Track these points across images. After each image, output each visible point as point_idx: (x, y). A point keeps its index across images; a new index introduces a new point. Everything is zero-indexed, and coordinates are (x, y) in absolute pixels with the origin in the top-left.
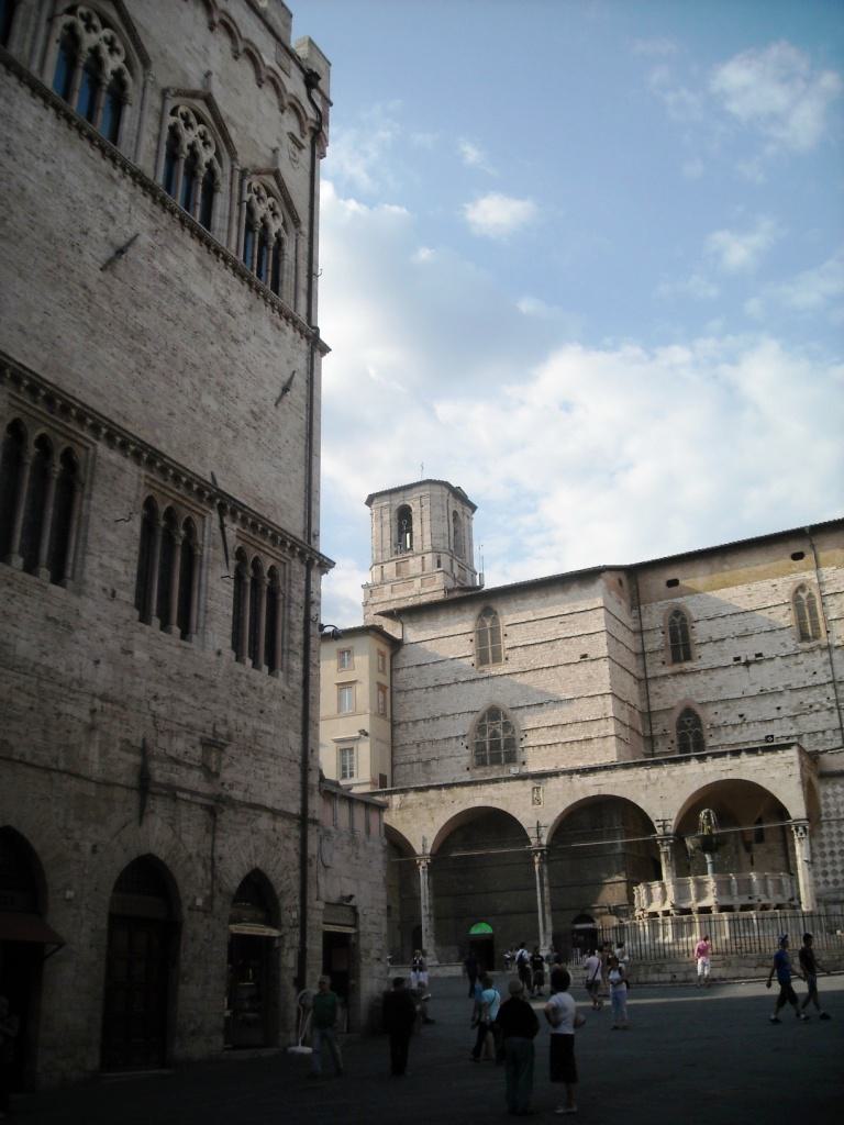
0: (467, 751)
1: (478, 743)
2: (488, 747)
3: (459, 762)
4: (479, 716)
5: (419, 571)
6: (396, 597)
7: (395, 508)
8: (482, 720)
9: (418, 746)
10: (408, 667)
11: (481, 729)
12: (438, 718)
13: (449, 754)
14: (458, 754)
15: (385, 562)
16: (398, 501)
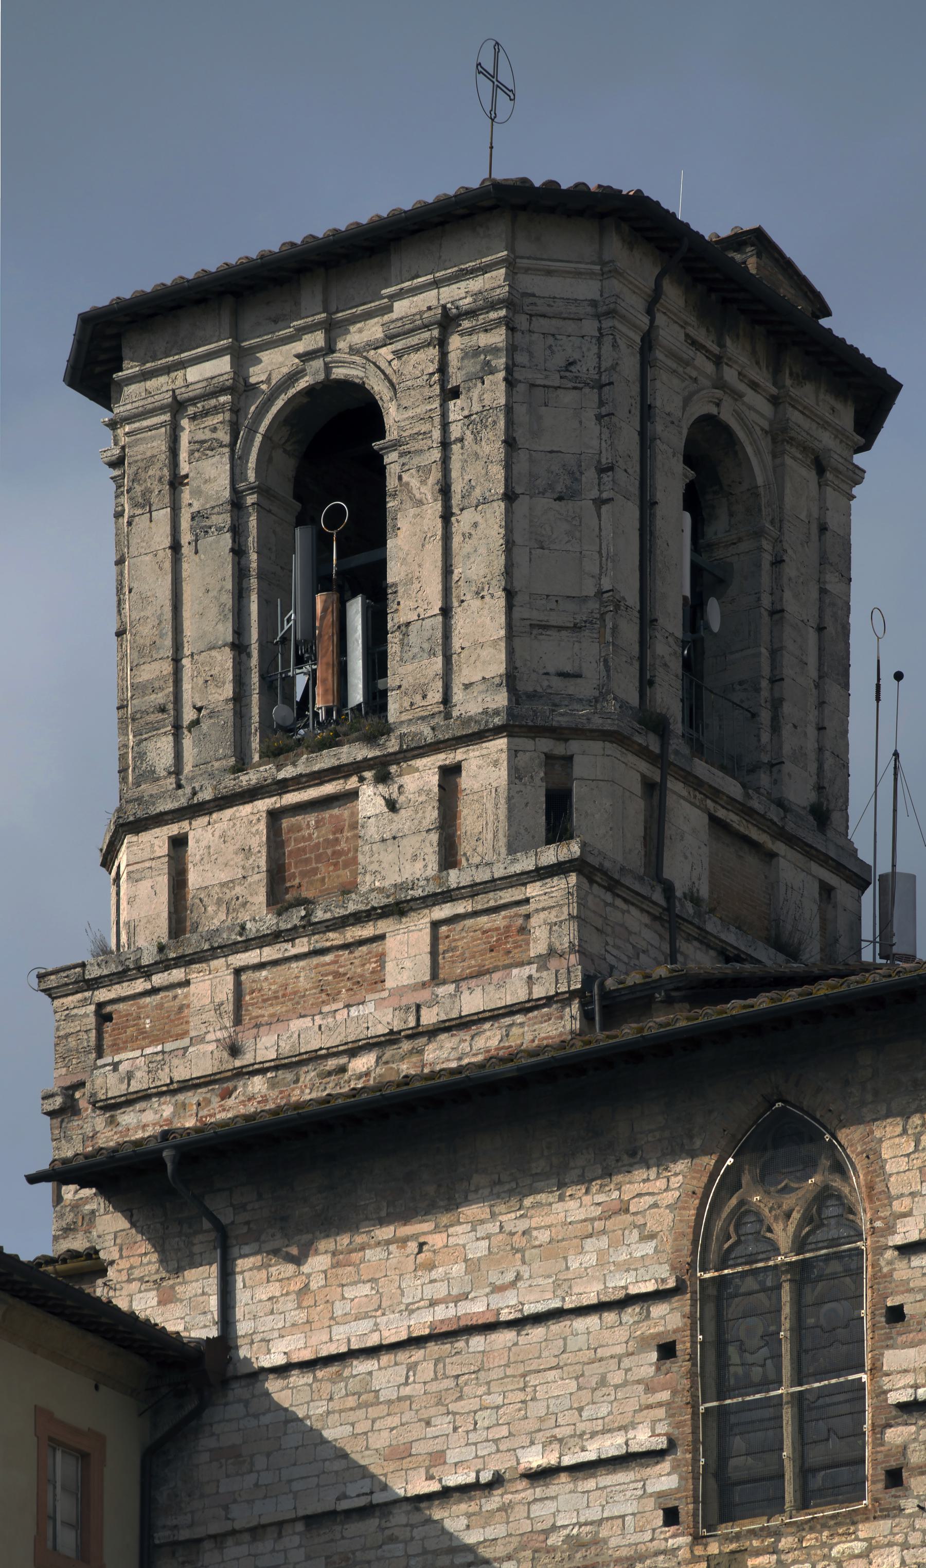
10: (256, 1531)
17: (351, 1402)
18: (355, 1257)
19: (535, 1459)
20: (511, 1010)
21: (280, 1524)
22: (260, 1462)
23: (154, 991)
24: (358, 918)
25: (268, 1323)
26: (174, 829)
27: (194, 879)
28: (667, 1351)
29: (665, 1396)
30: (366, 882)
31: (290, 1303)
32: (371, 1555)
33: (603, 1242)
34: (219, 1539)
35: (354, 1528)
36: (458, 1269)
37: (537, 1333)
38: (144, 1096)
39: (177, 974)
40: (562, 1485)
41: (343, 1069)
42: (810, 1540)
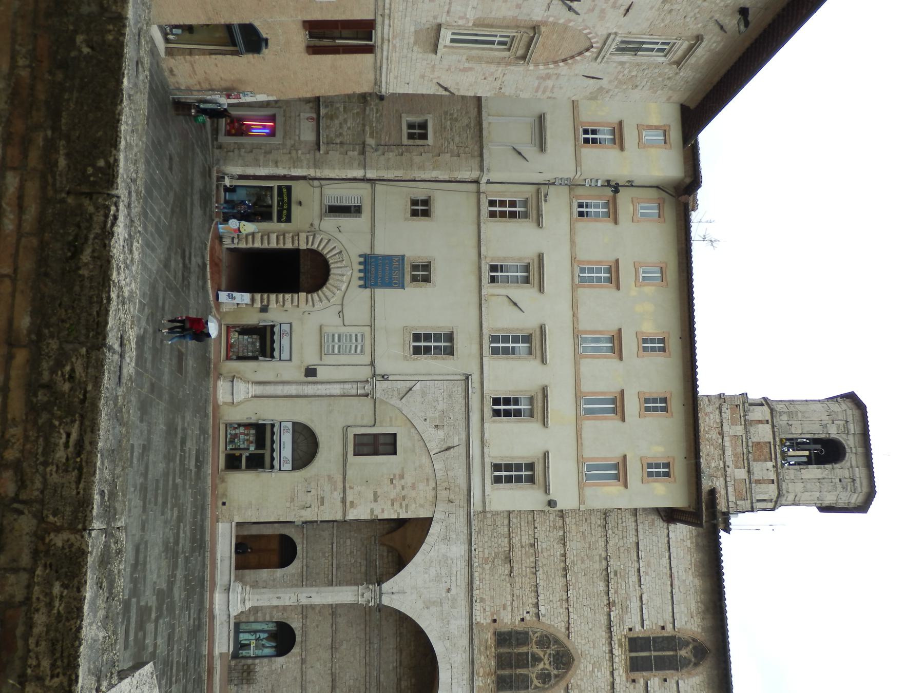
0: (518, 618)
1: (527, 633)
2: (520, 651)
3: (504, 608)
4: (562, 637)
5: (757, 475)
6: (727, 444)
7: (842, 438)
8: (557, 641)
9: (532, 545)
10: (637, 530)
11: (546, 640)
12: (565, 576)
13: (517, 592)
14: (515, 604)
15: (773, 426)
16: (851, 442)
17: (660, 553)
18: (689, 553)
19: (645, 598)
20: (728, 497)
21: (637, 536)
22: (650, 531)
23: (741, 417)
24: (749, 463)
25: (678, 531)
26: (770, 421)
27: (760, 425)
28: (663, 628)
29: (654, 628)
30: (755, 463)
31: (682, 538)
32: (629, 558)
33: (686, 612)
34: (636, 521)
35: (635, 554)
36: (684, 578)
37: (670, 598)
38: (721, 416)
39: (743, 423)
40: (639, 603)
41: (721, 460)
42: (623, 662)
